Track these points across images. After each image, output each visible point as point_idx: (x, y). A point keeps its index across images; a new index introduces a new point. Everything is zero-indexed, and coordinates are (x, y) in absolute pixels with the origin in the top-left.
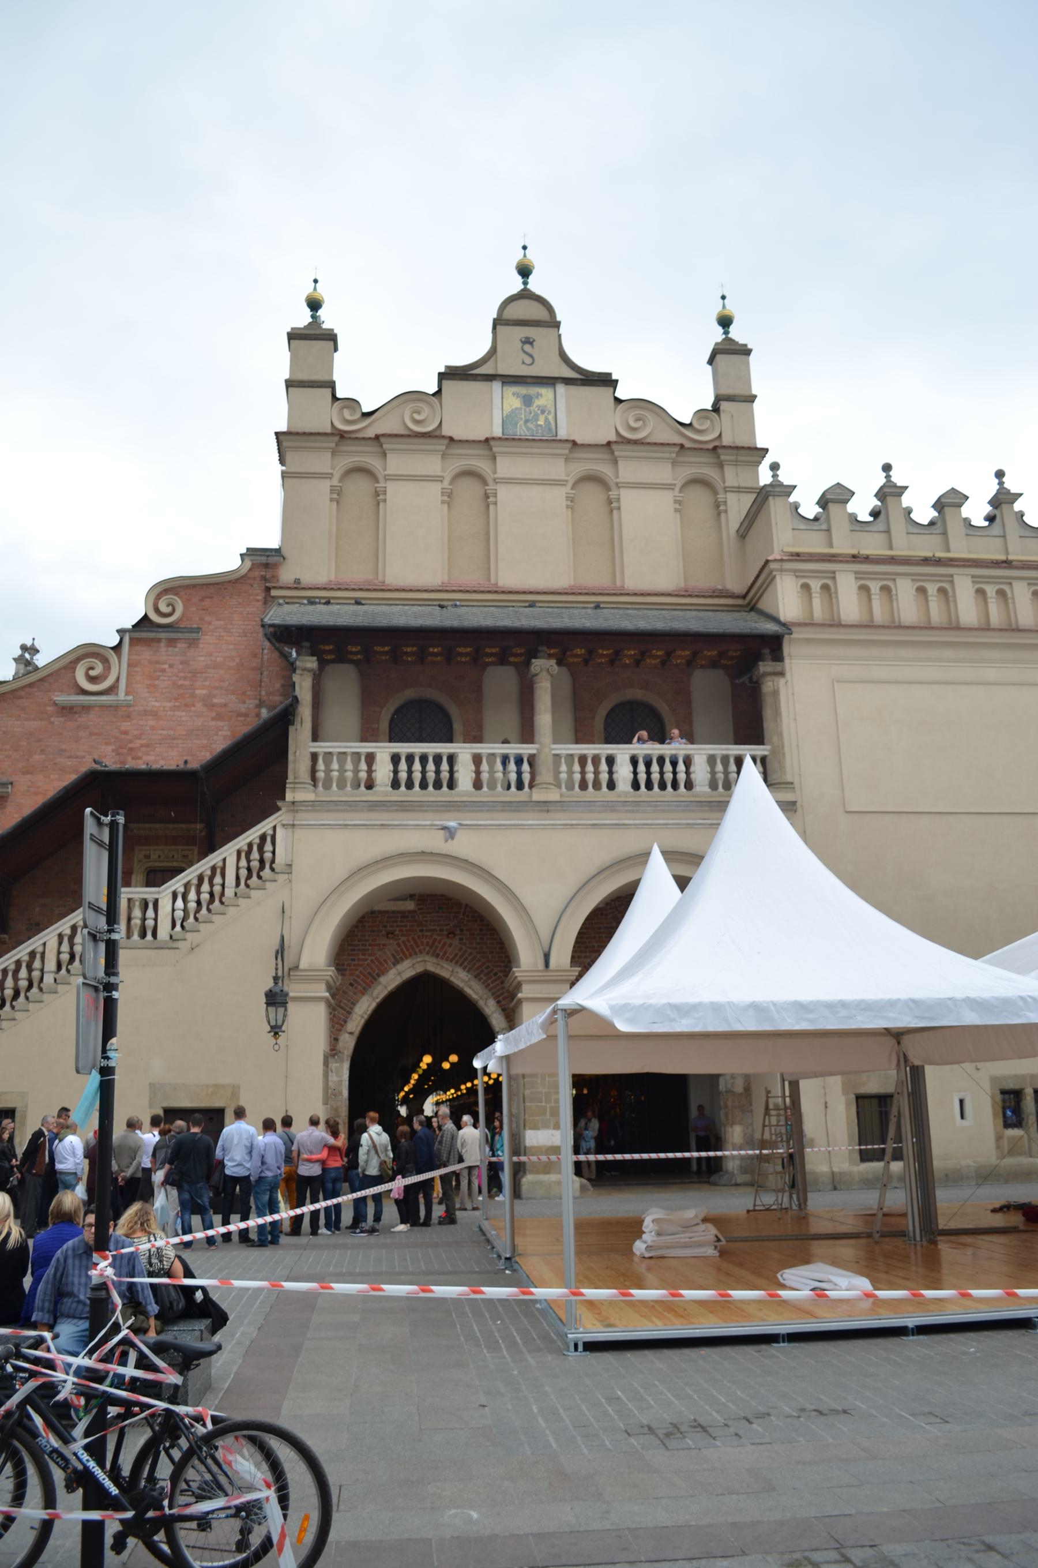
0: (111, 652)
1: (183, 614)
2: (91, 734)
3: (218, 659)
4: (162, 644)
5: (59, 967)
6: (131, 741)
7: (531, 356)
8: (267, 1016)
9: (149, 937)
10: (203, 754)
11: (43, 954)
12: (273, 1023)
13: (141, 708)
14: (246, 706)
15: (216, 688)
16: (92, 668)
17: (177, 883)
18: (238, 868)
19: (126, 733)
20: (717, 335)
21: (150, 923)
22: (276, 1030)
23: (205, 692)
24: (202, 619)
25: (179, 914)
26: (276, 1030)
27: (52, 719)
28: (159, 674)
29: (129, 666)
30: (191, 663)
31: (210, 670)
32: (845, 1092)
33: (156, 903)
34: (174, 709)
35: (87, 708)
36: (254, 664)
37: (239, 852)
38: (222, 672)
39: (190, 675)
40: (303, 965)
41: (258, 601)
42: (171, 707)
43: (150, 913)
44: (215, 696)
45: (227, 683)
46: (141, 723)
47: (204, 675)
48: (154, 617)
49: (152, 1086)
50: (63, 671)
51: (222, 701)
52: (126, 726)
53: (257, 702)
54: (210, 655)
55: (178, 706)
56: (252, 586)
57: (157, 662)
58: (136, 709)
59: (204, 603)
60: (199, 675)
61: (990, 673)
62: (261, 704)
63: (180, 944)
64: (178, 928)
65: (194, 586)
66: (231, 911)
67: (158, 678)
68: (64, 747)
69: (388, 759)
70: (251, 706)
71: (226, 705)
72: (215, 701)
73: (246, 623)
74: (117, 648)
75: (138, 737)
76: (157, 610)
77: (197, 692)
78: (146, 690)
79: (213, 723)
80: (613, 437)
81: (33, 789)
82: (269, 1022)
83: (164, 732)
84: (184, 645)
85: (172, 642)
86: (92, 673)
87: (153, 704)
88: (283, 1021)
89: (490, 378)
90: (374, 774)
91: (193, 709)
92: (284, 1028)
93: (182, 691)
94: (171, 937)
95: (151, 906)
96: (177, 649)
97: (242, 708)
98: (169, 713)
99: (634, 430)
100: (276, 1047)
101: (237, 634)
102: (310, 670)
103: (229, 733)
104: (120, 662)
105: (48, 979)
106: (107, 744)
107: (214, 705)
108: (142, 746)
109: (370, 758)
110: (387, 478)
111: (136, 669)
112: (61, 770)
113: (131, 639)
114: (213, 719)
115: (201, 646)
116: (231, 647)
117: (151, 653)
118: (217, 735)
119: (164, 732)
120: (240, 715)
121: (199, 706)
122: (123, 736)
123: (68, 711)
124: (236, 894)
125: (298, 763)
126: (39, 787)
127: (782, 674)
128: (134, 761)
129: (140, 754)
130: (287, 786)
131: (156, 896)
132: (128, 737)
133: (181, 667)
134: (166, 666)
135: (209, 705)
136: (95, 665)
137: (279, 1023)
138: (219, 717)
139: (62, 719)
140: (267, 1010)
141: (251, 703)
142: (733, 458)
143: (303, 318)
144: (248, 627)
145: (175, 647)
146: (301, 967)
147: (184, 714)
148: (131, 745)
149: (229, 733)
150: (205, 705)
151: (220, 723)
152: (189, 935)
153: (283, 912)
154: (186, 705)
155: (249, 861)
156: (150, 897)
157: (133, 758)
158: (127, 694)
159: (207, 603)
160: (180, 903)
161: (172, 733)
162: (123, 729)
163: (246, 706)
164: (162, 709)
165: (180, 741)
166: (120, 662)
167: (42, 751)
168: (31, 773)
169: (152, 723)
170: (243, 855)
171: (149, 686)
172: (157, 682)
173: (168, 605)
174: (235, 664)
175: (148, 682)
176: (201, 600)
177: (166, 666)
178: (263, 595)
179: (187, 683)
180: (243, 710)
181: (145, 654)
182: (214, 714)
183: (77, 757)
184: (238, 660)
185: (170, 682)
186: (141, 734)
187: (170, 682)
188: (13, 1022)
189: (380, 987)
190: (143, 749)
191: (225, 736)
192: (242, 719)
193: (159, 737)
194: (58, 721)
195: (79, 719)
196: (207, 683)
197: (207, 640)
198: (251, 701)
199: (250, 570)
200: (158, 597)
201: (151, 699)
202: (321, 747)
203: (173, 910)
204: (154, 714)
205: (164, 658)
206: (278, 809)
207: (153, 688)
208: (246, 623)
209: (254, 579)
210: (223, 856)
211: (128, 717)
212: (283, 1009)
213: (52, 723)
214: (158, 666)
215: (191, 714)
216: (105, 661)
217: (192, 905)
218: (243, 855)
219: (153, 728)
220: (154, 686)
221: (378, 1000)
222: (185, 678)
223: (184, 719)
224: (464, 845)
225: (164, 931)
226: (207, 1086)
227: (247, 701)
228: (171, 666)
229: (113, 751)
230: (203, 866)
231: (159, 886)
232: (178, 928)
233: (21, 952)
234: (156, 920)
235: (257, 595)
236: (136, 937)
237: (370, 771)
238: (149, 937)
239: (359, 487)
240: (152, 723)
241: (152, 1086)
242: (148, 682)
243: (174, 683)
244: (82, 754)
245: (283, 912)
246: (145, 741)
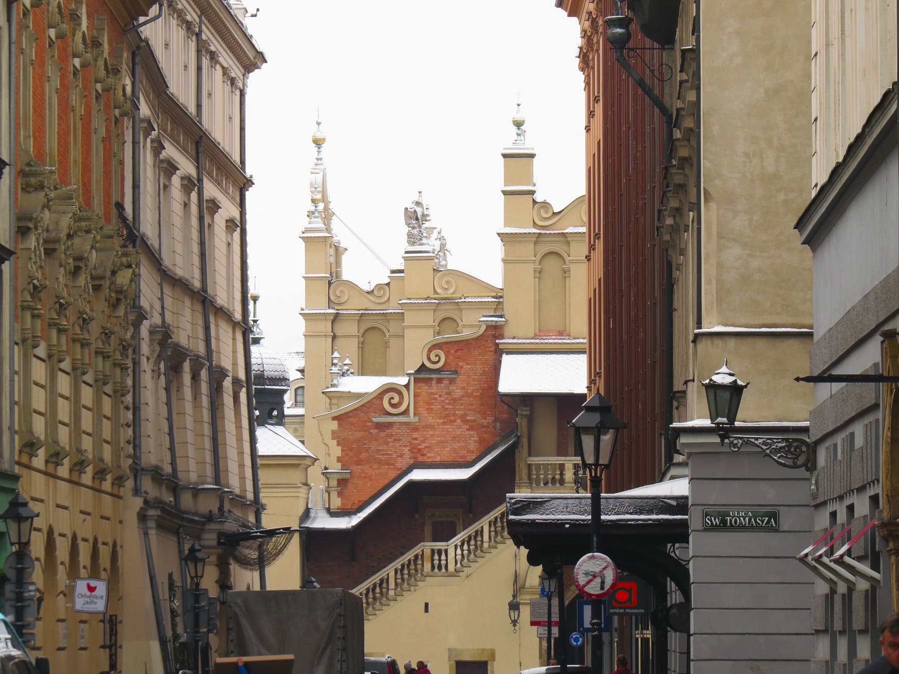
0: (404, 388)
1: (446, 361)
2: (395, 440)
3: (469, 391)
4: (434, 382)
5: (396, 584)
6: (419, 444)
8: (510, 615)
9: (443, 570)
10: (462, 452)
11: (388, 580)
12: (513, 619)
13: (424, 424)
14: (487, 421)
15: (469, 410)
16: (392, 398)
17: (457, 539)
18: (490, 532)
19: (416, 439)
21: (443, 562)
22: (514, 623)
23: (462, 412)
24: (457, 365)
25: (459, 557)
26: (514, 623)
27: (371, 431)
28: (433, 401)
29: (415, 396)
30: (453, 394)
31: (464, 399)
33: (446, 551)
34: (444, 423)
35: (390, 425)
36: (491, 394)
37: (490, 523)
38: (471, 399)
39: (452, 402)
40: (527, 585)
41: (491, 351)
42: (442, 423)
43: (443, 557)
44: (468, 415)
45: (475, 407)
46: (424, 433)
47: (461, 402)
48: (428, 364)
49: (449, 650)
50: (375, 400)
51: (473, 418)
52: (415, 435)
53: (493, 418)
54: (463, 388)
55: (446, 422)
56: (487, 341)
57: (431, 394)
58: (421, 424)
59: (458, 354)
60: (457, 402)
62: (496, 420)
63: (461, 574)
64: (459, 565)
66: (487, 555)
67: (432, 404)
68: (379, 448)
69: (571, 466)
70: (490, 421)
71: (475, 421)
72: (468, 418)
73: (485, 366)
74: (407, 386)
75: (424, 441)
76: (429, 359)
77: (457, 412)
78: (426, 412)
79: (467, 433)
81: (363, 475)
82: (511, 618)
83: (439, 439)
84: (447, 382)
85: (439, 381)
86: (393, 402)
87: (431, 420)
88: (518, 618)
90: (564, 477)
91: (455, 423)
92: (518, 622)
93: (448, 413)
94: (455, 570)
95: (443, 553)
96: (443, 385)
97: (485, 422)
98: (441, 426)
100: (515, 631)
101: (479, 374)
102: (526, 415)
103: (477, 439)
104: (409, 394)
105: (391, 593)
106: (405, 446)
107: (468, 421)
108: (426, 447)
109: (562, 467)
110: (571, 262)
111: (419, 398)
112: (378, 463)
113: (415, 378)
114: (468, 430)
115: (457, 382)
116: (476, 382)
117: (427, 387)
118: (470, 440)
119: (439, 439)
120: (483, 427)
121: (459, 421)
122: (414, 442)
123: (379, 426)
124: (489, 546)
125: (522, 472)
126: (367, 473)
128: (422, 457)
129: (425, 453)
130: (516, 485)
131: (446, 548)
132: (416, 442)
133: (446, 396)
134: (437, 396)
135: (465, 421)
136: (395, 397)
137: (516, 618)
138: (471, 429)
139: (377, 431)
140: (509, 612)
141: (490, 419)
144: (486, 369)
145: (442, 383)
146: (526, 586)
147: (450, 427)
148: (419, 447)
149: (477, 439)
150: (462, 421)
151: (471, 433)
152: (465, 569)
153: (516, 556)
154: (451, 421)
155: (496, 527)
156: (443, 548)
157: (421, 455)
158: (415, 414)
159: (460, 353)
160: (459, 551)
161: (443, 439)
162: (414, 436)
163: (487, 421)
164: (436, 424)
165: (448, 444)
166: (409, 394)
167: (367, 451)
168: (361, 465)
169: (431, 433)
170: (492, 524)
171: (428, 409)
172: (432, 407)
173: (436, 356)
174: (479, 394)
175: (427, 407)
176: (456, 352)
177: (437, 396)
178: (494, 347)
179: (451, 407)
180: (485, 424)
181: (424, 388)
182: (468, 427)
183: (388, 454)
184: (481, 391)
185: (440, 407)
186: (425, 440)
187: (440, 407)
188: (375, 616)
189: (571, 592)
190: (427, 449)
191: (475, 441)
192: (485, 429)
193: (436, 442)
194: (374, 431)
195: (387, 431)
196: (463, 407)
197: (461, 380)
198: (490, 418)
199: (486, 330)
200: (430, 351)
201: (429, 418)
202: (535, 460)
203: (456, 555)
204: (432, 427)
205: (436, 391)
207: (429, 410)
208: (485, 366)
209: (488, 336)
210: (481, 525)
211: (417, 429)
212: (518, 611)
213: (371, 433)
214: (432, 396)
215: (454, 427)
216: (400, 393)
217: (466, 552)
218: (492, 524)
219: (432, 436)
220: (431, 409)
221: (570, 600)
222: (449, 404)
223: (450, 430)
225: (451, 568)
226: (478, 649)
227: (487, 418)
228: (440, 396)
229: (409, 450)
230: (471, 530)
231: (447, 541)
232: (459, 565)
233: (376, 578)
234: (447, 560)
235: (491, 347)
236: (436, 570)
237: (562, 474)
238: (443, 570)
239: (552, 265)
240: (431, 433)
241: (449, 650)
242: (427, 407)
243: (442, 407)
244: (391, 453)
245: (516, 556)
246: (427, 445)
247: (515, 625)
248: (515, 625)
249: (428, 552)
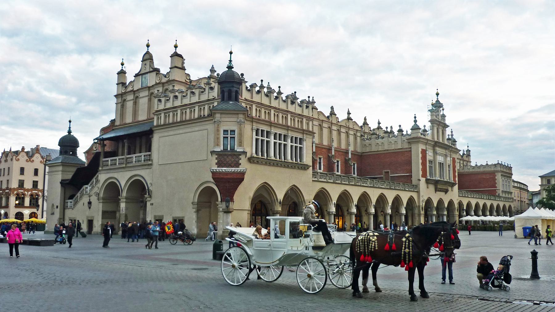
7: (146, 68)
17: (89, 185)
20: (173, 50)
22: (90, 208)
26: (90, 208)
32: (154, 219)
61: (181, 131)
65: (105, 128)
80: (154, 83)
89: (140, 75)
99: (159, 80)
105: (79, 200)
127: (153, 137)
142: (170, 83)
143: (119, 68)
206: (98, 171)
224: (115, 175)
225: (88, 192)
247: (90, 209)
248: (90, 209)
249: (85, 188)
